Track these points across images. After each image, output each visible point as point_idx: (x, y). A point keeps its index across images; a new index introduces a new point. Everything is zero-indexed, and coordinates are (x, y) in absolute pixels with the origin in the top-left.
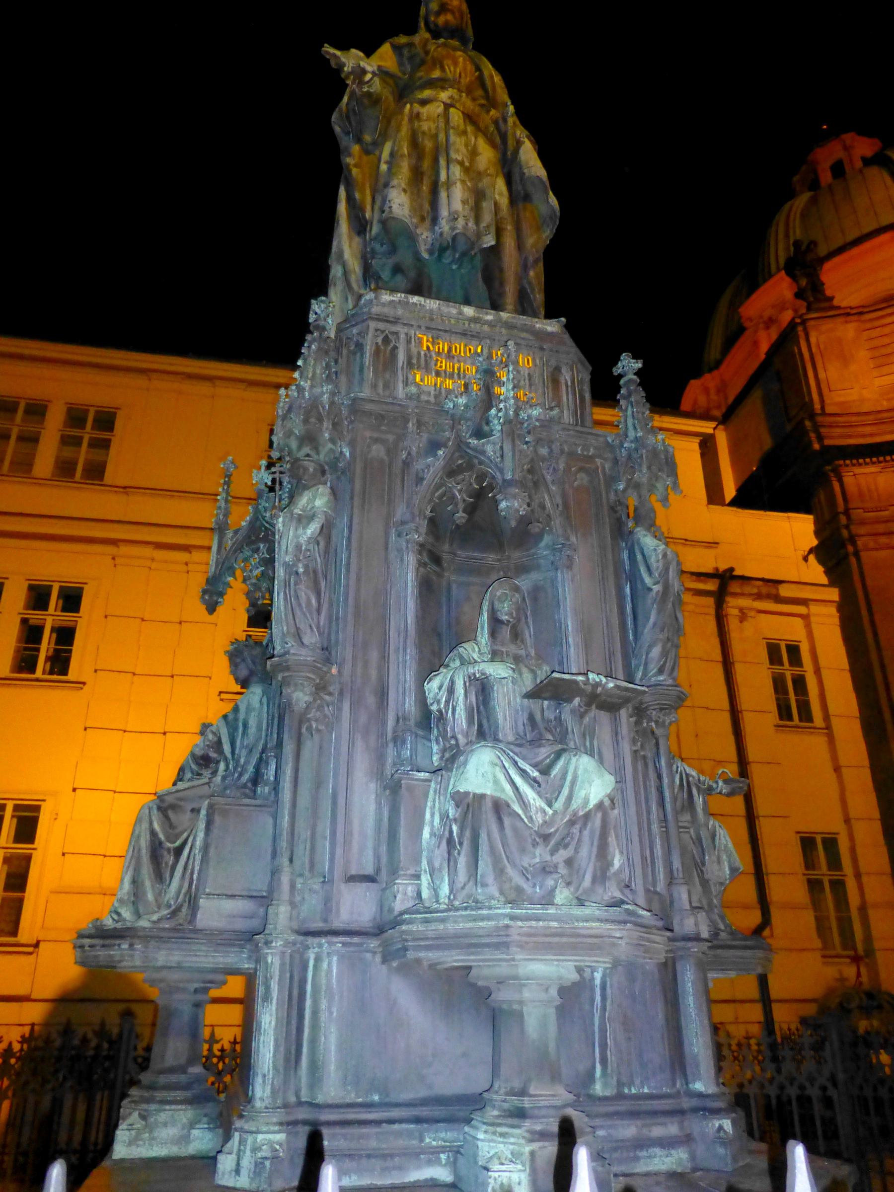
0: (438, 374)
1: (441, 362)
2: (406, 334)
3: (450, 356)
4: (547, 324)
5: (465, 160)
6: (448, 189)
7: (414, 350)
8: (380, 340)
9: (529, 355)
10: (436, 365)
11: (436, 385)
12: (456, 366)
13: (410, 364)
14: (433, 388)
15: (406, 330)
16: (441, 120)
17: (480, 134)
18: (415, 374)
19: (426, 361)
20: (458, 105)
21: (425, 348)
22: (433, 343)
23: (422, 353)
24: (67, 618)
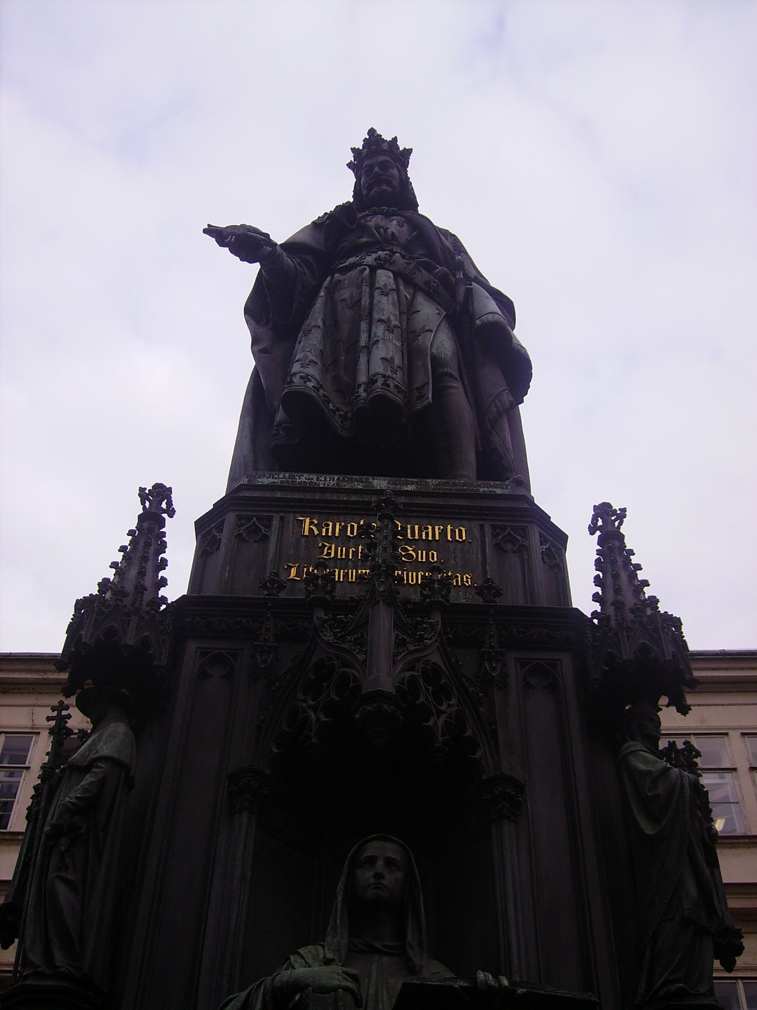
1: (330, 548)
2: (282, 519)
3: (343, 540)
4: (495, 486)
5: (392, 318)
6: (369, 354)
20: (386, 266)
21: (306, 533)
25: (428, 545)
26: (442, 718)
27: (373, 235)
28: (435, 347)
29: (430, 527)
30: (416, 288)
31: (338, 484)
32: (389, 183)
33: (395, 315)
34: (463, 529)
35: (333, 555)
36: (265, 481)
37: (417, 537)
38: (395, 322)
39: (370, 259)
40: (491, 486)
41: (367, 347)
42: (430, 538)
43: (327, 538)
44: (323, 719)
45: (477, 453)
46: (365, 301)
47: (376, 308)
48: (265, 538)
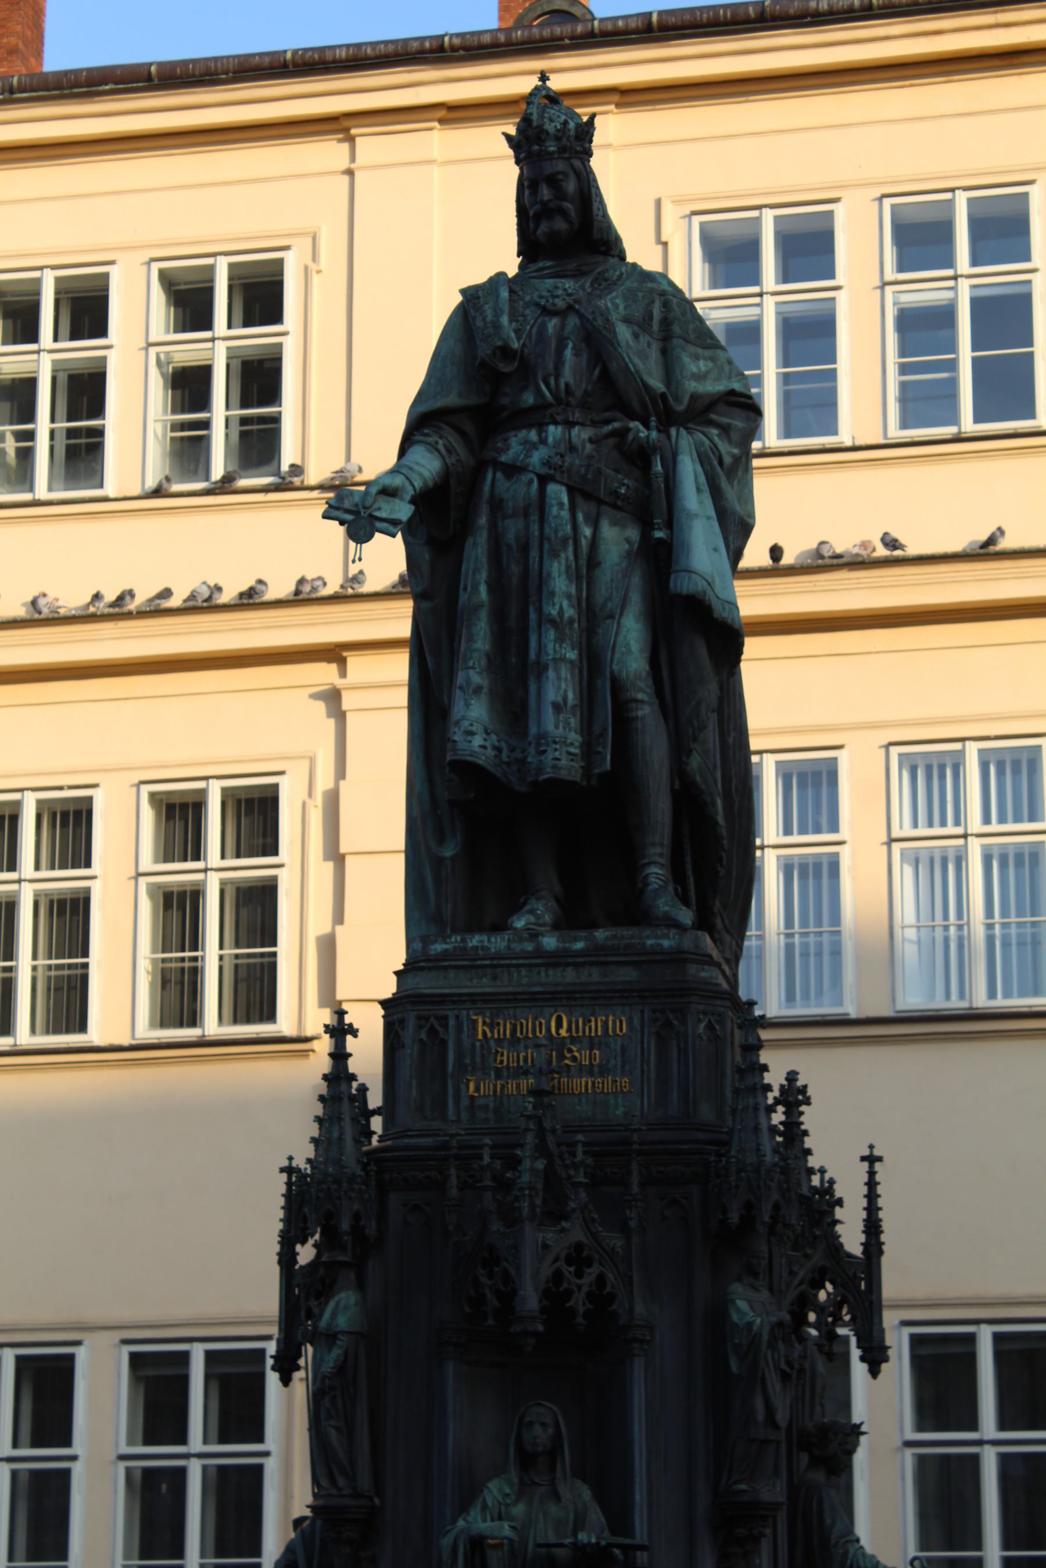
0: (499, 1074)
1: (502, 1055)
2: (457, 1017)
3: (514, 1041)
7: (466, 1042)
8: (423, 1036)
9: (623, 1013)
10: (495, 1060)
11: (495, 1091)
12: (522, 1055)
13: (460, 1065)
14: (492, 1099)
15: (456, 1012)
16: (534, 517)
17: (605, 508)
18: (469, 1081)
19: (483, 1056)
20: (558, 477)
21: (480, 1037)
22: (492, 1026)
23: (478, 1044)
24: (252, 868)
25: (592, 1043)
26: (585, 1289)
27: (539, 393)
28: (617, 656)
29: (593, 1019)
30: (600, 502)
31: (509, 948)
32: (563, 213)
33: (569, 596)
34: (623, 1019)
35: (505, 1063)
36: (438, 947)
37: (581, 1034)
38: (570, 612)
39: (536, 458)
40: (657, 937)
41: (538, 662)
42: (593, 1034)
43: (499, 1041)
44: (496, 1304)
45: (674, 793)
46: (534, 554)
47: (545, 588)
48: (444, 1042)
